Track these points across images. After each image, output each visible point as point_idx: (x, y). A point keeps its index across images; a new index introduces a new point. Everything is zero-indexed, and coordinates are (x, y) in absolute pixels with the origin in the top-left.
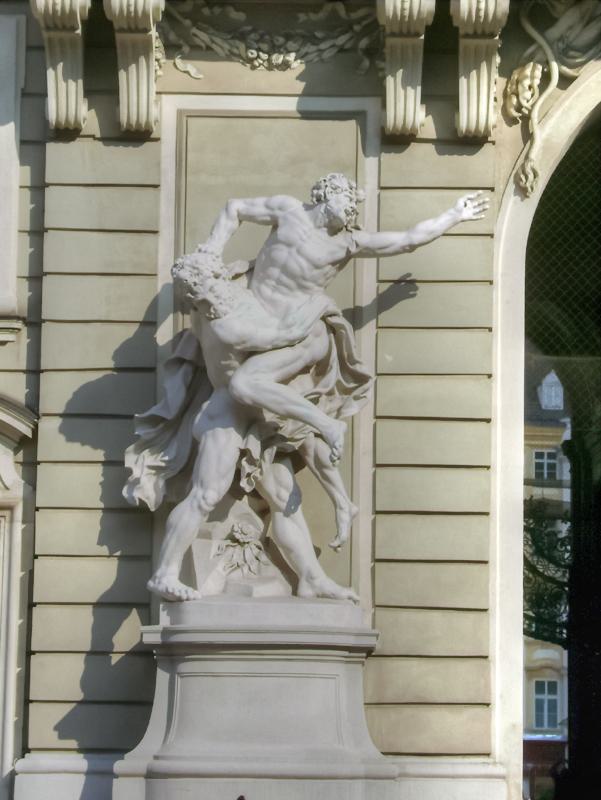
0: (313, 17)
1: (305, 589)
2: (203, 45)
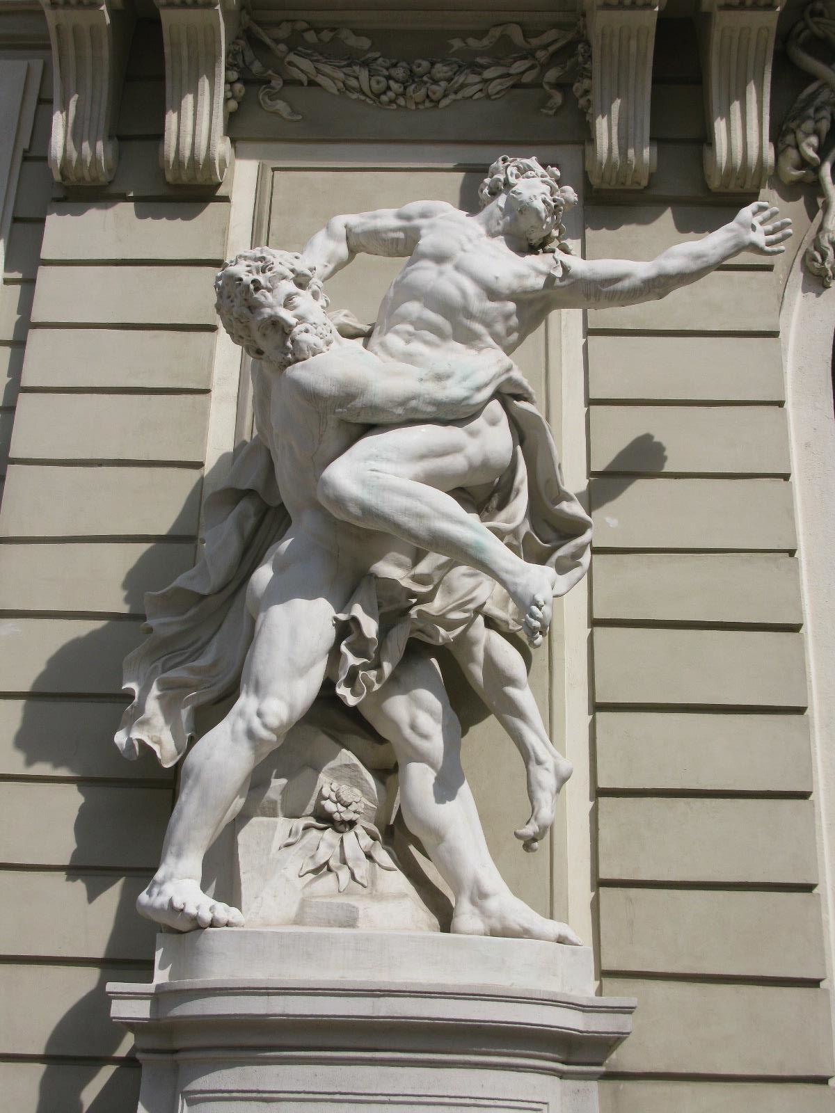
0: (471, 41)
1: (466, 916)
2: (304, 79)
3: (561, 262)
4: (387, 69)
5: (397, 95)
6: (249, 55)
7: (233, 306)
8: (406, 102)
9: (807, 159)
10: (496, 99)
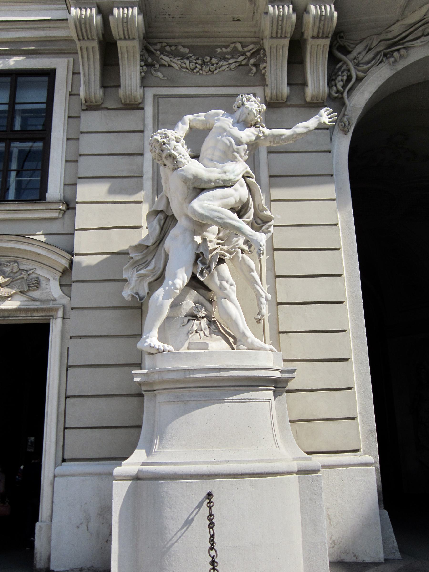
0: (224, 49)
2: (166, 64)
3: (262, 131)
4: (195, 60)
5: (199, 69)
6: (147, 55)
7: (156, 150)
8: (202, 72)
9: (339, 90)
10: (233, 70)
